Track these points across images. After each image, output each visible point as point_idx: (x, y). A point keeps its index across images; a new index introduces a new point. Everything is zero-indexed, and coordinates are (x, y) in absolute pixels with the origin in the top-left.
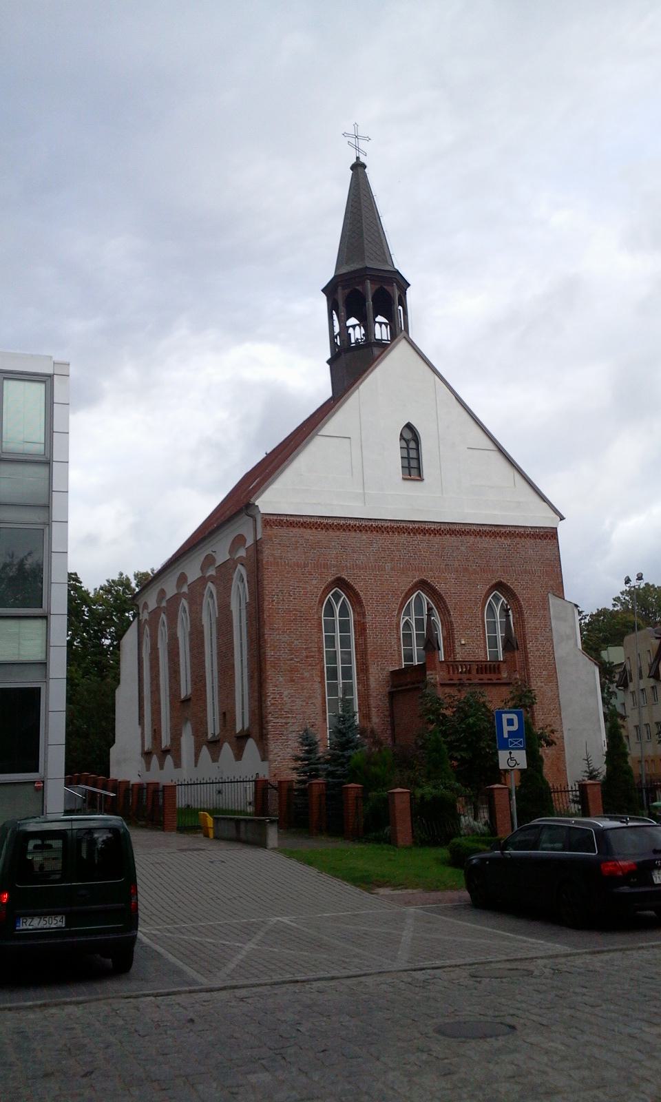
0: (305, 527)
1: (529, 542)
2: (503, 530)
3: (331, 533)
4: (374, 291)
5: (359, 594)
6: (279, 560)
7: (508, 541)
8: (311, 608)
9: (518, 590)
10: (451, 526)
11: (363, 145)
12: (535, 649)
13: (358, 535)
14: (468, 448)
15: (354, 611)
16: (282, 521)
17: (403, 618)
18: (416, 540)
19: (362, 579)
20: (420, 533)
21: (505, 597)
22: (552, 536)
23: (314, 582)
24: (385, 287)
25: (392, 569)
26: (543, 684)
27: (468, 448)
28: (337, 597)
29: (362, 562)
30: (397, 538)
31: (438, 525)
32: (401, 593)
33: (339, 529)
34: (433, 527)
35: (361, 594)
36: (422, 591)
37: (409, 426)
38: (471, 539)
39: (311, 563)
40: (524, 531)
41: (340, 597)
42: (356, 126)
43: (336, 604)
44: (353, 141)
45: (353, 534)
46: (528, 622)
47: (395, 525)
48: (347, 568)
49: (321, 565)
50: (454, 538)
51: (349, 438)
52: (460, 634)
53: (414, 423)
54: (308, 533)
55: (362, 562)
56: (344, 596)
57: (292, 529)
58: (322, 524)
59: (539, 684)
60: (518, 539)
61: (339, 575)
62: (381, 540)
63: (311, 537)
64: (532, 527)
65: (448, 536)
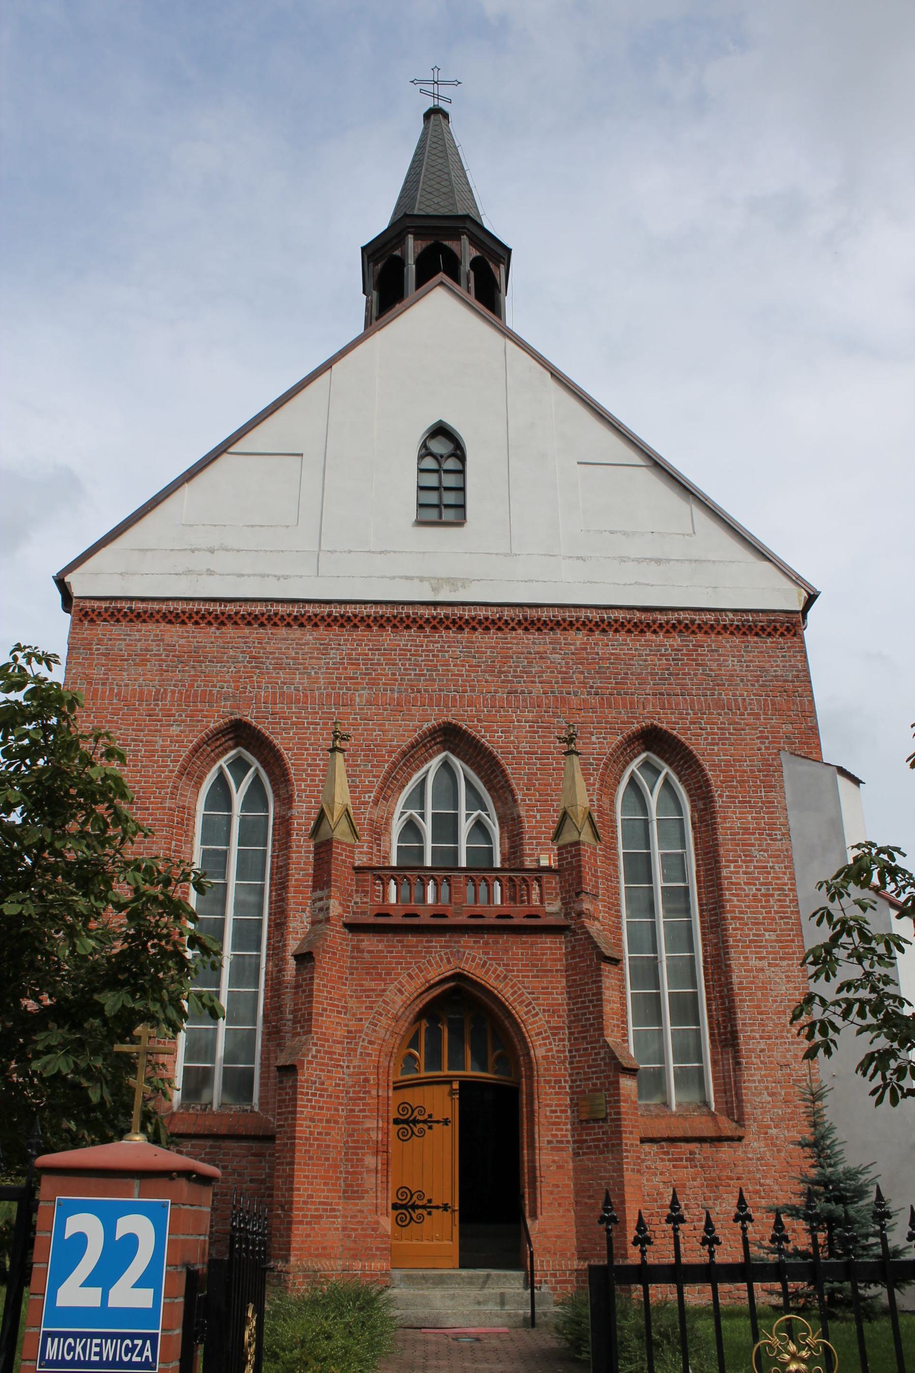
0: (170, 622)
1: (729, 642)
2: (661, 618)
3: (229, 631)
4: (419, 250)
5: (281, 755)
6: (100, 686)
7: (676, 640)
8: (160, 785)
9: (698, 746)
10: (529, 612)
11: (444, 91)
12: (743, 878)
13: (296, 633)
14: (578, 463)
15: (276, 795)
16: (119, 611)
17: (403, 813)
18: (437, 642)
19: (293, 723)
20: (447, 628)
21: (670, 765)
22: (788, 629)
23: (175, 730)
24: (446, 243)
25: (369, 703)
26: (765, 963)
27: (578, 463)
28: (239, 767)
29: (297, 689)
30: (388, 638)
31: (495, 609)
32: (390, 753)
33: (249, 624)
34: (482, 613)
35: (286, 755)
36: (453, 752)
37: (440, 431)
38: (579, 638)
39: (173, 692)
40: (717, 620)
41: (250, 767)
42: (436, 70)
43: (238, 785)
44: (429, 88)
45: (283, 632)
46: (725, 818)
47: (388, 611)
48: (258, 701)
49: (196, 696)
50: (533, 636)
51: (302, 455)
52: (538, 844)
53: (453, 422)
54: (174, 634)
55: (297, 689)
56: (256, 764)
57: (140, 626)
58: (210, 613)
59: (753, 962)
60: (700, 636)
61: (238, 717)
62: (345, 643)
63: (182, 641)
64: (735, 611)
65: (520, 631)
